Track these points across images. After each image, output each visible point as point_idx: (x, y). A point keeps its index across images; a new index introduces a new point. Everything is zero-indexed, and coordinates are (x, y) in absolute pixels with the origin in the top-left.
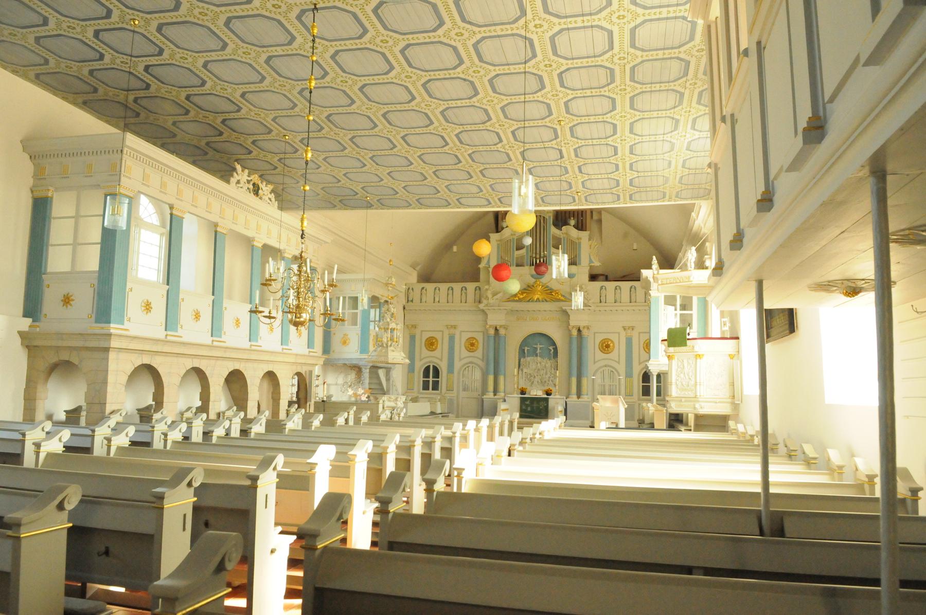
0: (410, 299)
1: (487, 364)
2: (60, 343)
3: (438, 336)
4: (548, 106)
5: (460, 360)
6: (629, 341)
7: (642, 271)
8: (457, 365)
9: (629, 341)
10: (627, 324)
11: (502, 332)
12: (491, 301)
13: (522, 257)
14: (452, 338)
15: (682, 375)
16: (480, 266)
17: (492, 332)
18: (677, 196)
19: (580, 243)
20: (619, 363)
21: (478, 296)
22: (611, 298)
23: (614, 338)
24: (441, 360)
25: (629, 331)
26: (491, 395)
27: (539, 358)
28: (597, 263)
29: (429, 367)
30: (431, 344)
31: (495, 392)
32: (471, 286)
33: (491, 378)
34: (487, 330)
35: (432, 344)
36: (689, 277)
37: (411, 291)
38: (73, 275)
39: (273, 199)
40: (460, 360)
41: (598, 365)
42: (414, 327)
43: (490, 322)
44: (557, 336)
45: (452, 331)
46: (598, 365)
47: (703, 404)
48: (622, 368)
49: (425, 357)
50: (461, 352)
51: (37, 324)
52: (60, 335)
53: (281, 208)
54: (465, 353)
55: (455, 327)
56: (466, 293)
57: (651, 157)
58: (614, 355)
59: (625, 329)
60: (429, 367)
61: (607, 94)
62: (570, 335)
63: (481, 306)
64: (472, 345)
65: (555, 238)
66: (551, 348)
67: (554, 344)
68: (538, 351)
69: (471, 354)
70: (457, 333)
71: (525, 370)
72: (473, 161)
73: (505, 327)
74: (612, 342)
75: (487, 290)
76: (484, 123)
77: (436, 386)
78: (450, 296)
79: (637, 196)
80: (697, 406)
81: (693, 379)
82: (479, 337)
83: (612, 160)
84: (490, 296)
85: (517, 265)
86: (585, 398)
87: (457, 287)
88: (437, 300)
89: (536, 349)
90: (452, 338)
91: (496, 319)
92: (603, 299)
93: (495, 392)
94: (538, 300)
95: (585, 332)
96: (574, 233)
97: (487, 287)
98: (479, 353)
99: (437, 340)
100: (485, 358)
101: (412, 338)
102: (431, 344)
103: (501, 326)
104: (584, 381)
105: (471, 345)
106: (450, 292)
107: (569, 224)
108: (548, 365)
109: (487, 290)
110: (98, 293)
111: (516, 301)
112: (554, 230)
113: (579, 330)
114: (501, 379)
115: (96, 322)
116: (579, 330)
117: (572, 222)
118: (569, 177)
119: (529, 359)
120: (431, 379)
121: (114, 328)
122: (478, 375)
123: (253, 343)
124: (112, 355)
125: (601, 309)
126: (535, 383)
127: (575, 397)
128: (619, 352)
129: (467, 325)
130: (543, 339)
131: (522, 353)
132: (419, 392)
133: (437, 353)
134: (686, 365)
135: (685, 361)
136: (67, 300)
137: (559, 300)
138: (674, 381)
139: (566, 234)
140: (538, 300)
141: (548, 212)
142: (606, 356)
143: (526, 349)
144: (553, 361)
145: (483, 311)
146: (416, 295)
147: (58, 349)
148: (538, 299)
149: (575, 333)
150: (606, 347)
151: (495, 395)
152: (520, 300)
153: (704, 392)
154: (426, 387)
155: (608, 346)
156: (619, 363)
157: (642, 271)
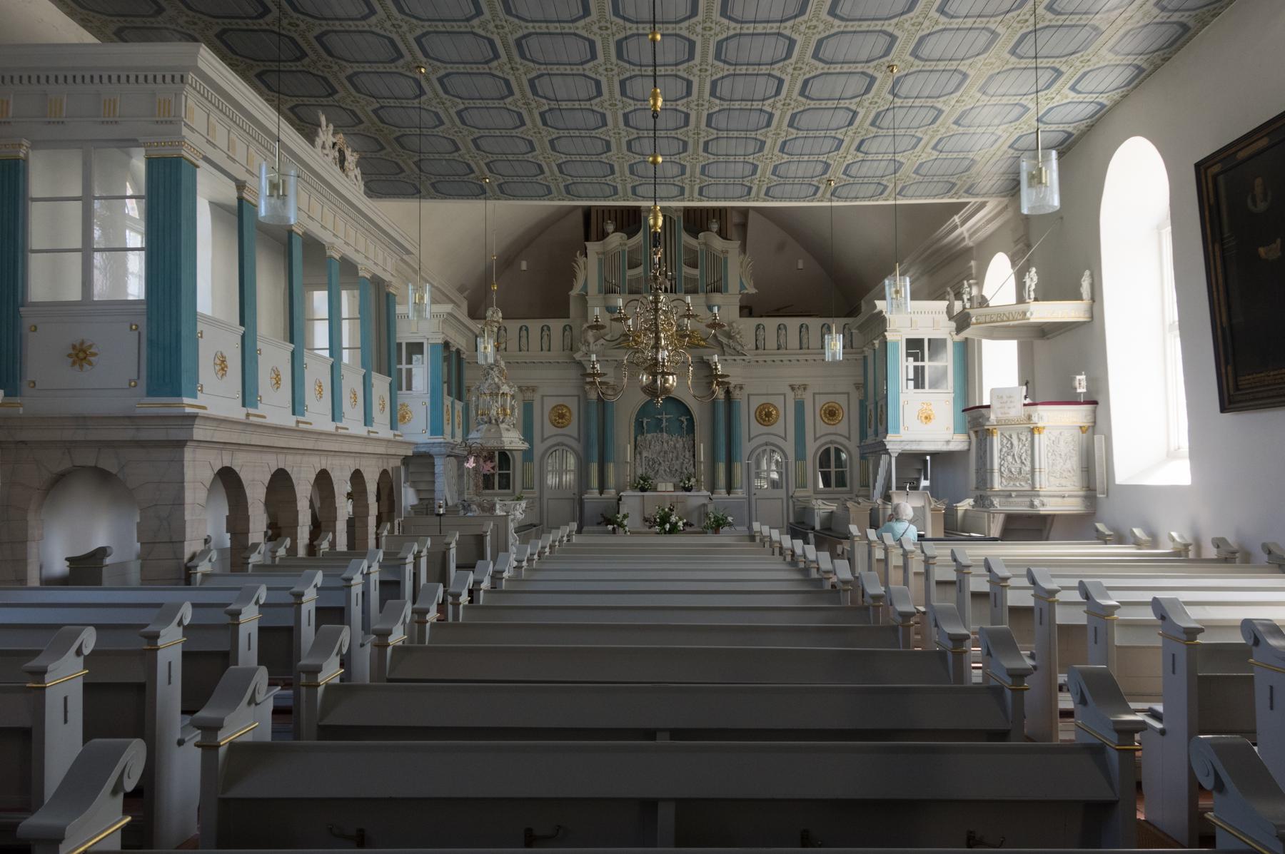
1: (587, 447)
2: (80, 435)
4: (592, 44)
5: (543, 440)
6: (800, 406)
7: (877, 302)
9: (800, 406)
10: (797, 382)
13: (638, 280)
15: (1010, 458)
16: (573, 293)
18: (966, 192)
19: (726, 259)
20: (785, 439)
22: (771, 342)
23: (778, 402)
28: (752, 291)
31: (602, 487)
32: (557, 325)
33: (594, 468)
34: (585, 393)
36: (1025, 314)
38: (88, 307)
39: (359, 178)
40: (543, 440)
41: (755, 443)
45: (529, 395)
46: (755, 443)
47: (1045, 500)
51: (18, 400)
52: (82, 420)
53: (372, 191)
54: (550, 430)
55: (534, 390)
56: (549, 336)
57: (817, 133)
58: (778, 428)
59: (792, 388)
61: (733, 25)
64: (562, 416)
66: (683, 419)
67: (687, 411)
68: (664, 424)
69: (560, 431)
70: (537, 397)
71: (645, 454)
72: (463, 122)
76: (487, 62)
78: (524, 340)
79: (844, 192)
80: (1036, 502)
81: (1028, 463)
82: (573, 404)
83: (680, 134)
84: (591, 340)
85: (631, 293)
87: (535, 326)
89: (661, 420)
92: (760, 344)
93: (602, 487)
95: (736, 394)
96: (718, 243)
98: (572, 429)
105: (559, 417)
106: (524, 333)
107: (708, 230)
110: (151, 342)
112: (686, 238)
114: (611, 469)
115: (151, 392)
117: (715, 227)
118: (613, 156)
119: (649, 436)
121: (188, 404)
122: (571, 461)
123: (339, 425)
124: (188, 454)
125: (760, 359)
127: (722, 492)
128: (785, 424)
131: (640, 428)
134: (1015, 442)
135: (1015, 437)
136: (81, 355)
138: (996, 466)
139: (705, 244)
141: (677, 209)
142: (765, 429)
143: (645, 421)
147: (69, 446)
151: (601, 493)
153: (1046, 483)
155: (769, 415)
156: (785, 439)
157: (877, 302)
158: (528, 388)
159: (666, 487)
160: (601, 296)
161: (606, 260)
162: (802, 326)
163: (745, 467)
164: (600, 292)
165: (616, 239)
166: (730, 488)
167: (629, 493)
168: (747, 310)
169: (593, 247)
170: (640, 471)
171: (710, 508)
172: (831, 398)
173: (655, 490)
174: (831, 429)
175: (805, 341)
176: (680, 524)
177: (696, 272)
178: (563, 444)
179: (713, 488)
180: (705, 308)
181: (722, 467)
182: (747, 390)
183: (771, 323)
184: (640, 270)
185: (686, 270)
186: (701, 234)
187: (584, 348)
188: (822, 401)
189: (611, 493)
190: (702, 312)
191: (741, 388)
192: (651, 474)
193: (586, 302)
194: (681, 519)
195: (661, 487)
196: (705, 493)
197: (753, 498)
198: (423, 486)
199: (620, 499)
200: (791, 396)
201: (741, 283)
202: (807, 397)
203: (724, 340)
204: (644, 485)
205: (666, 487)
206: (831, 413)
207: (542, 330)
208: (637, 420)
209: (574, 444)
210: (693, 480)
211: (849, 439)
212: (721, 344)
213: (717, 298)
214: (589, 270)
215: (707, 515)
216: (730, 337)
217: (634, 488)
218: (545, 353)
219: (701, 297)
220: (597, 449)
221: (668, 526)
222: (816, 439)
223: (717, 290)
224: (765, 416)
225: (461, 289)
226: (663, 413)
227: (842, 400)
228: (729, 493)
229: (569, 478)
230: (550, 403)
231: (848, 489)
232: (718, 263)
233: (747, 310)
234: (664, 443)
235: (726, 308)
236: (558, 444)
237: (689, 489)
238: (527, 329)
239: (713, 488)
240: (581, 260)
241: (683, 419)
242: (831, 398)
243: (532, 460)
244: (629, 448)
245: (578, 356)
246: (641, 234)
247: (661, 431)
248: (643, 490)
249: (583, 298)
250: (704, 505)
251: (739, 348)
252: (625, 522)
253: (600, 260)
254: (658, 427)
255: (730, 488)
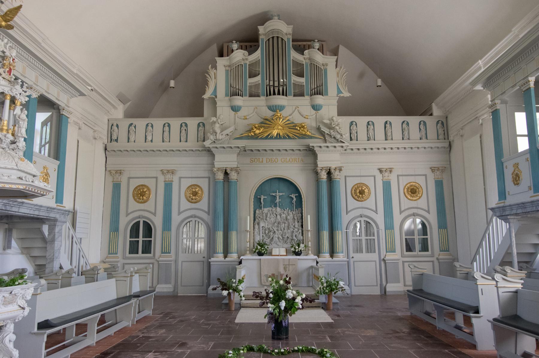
0: (114, 137)
3: (151, 184)
5: (180, 213)
6: (387, 186)
8: (176, 219)
9: (387, 186)
10: (384, 166)
11: (233, 176)
12: (219, 136)
13: (257, 86)
14: (168, 186)
16: (205, 96)
17: (220, 176)
19: (326, 70)
20: (376, 212)
21: (201, 134)
23: (370, 182)
24: (155, 214)
25: (386, 174)
26: (219, 257)
27: (278, 209)
28: (346, 94)
29: (138, 223)
30: (141, 194)
31: (226, 252)
32: (193, 123)
33: (220, 236)
35: (142, 194)
37: (115, 128)
40: (180, 213)
41: (352, 215)
42: (120, 172)
43: (217, 165)
44: (301, 180)
45: (169, 177)
46: (352, 215)
48: (380, 218)
49: (132, 211)
50: (180, 203)
54: (185, 204)
55: (173, 172)
56: (186, 131)
58: (370, 203)
59: (381, 171)
60: (138, 223)
62: (318, 181)
63: (207, 144)
64: (195, 194)
65: (296, 64)
66: (293, 196)
67: (296, 190)
69: (194, 206)
70: (175, 179)
71: (262, 224)
73: (237, 170)
74: (367, 186)
75: (214, 123)
77: (147, 248)
78: (166, 134)
82: (204, 184)
84: (218, 131)
85: (251, 96)
86: (341, 257)
87: (175, 123)
88: (149, 138)
89: (275, 197)
90: (168, 186)
91: (225, 160)
93: (226, 252)
94: (278, 137)
95: (336, 175)
96: (319, 58)
97: (214, 119)
98: (204, 204)
99: (149, 189)
100: (212, 211)
101: (117, 187)
102: (141, 194)
103: (232, 169)
104: (340, 237)
105: (194, 194)
106: (167, 128)
108: (290, 217)
109: (214, 123)
111: (252, 138)
112: (294, 55)
113: (329, 173)
114: (234, 236)
116: (329, 173)
117: (317, 45)
119: (266, 210)
120: (141, 239)
122: (202, 232)
126: (275, 239)
127: (326, 256)
128: (375, 200)
129: (189, 171)
130: (282, 186)
131: (258, 203)
132: (125, 258)
133: (149, 206)
137: (304, 136)
139: (310, 59)
140: (278, 137)
142: (359, 204)
143: (262, 198)
144: (296, 212)
145: (209, 151)
146: (122, 134)
148: (278, 134)
149: (324, 176)
150: (360, 193)
151: (225, 257)
152: (256, 137)
154: (134, 249)
155: (362, 192)
158: (168, 171)
159: (279, 251)
160: (227, 98)
161: (235, 71)
162: (386, 123)
163: (344, 235)
164: (227, 95)
165: (239, 55)
166: (332, 253)
167: (249, 256)
168: (344, 110)
169: (222, 62)
170: (258, 238)
171: (321, 273)
172: (412, 179)
173: (270, 254)
174: (414, 204)
175: (389, 134)
176: (298, 300)
177: (302, 80)
178: (195, 217)
179: (318, 252)
180: (310, 108)
181: (325, 235)
182: (344, 173)
183: (362, 121)
184: (258, 79)
185: (295, 79)
186: (306, 52)
187: (212, 137)
188: (404, 181)
189: (233, 257)
190: (308, 111)
191: (340, 170)
192: (268, 241)
193: (216, 103)
194: (299, 294)
195: (275, 251)
196: (312, 256)
197: (352, 261)
198: (36, 253)
199: (240, 263)
200: (379, 177)
201: (338, 88)
202: (393, 178)
203: (326, 131)
204: (261, 250)
205: (279, 251)
206: (413, 191)
207: (181, 126)
208: (256, 197)
209: (205, 216)
210: (302, 246)
211: (428, 212)
212: (322, 134)
213: (319, 100)
214: (219, 79)
215: (317, 278)
216: (330, 127)
217: (253, 252)
218: (183, 144)
219: (305, 101)
220: (223, 220)
221: (283, 304)
222: (401, 212)
223: (320, 93)
224: (360, 193)
225: (122, 99)
226: (278, 192)
227: (421, 181)
228: (332, 256)
229: (201, 245)
230: (186, 183)
231: (429, 253)
232: (318, 72)
233: (344, 110)
234: (278, 216)
235: (329, 105)
236: (191, 217)
237: (298, 254)
238: (169, 126)
239: (318, 252)
240: (212, 72)
241: (293, 196)
242: (412, 179)
243: (169, 229)
244: (249, 220)
245: (207, 144)
246: (259, 52)
247: (275, 206)
248: (260, 254)
249: (213, 101)
250: (312, 267)
251: (338, 137)
252: (240, 288)
253: (227, 71)
254: (273, 203)
255: (332, 253)
